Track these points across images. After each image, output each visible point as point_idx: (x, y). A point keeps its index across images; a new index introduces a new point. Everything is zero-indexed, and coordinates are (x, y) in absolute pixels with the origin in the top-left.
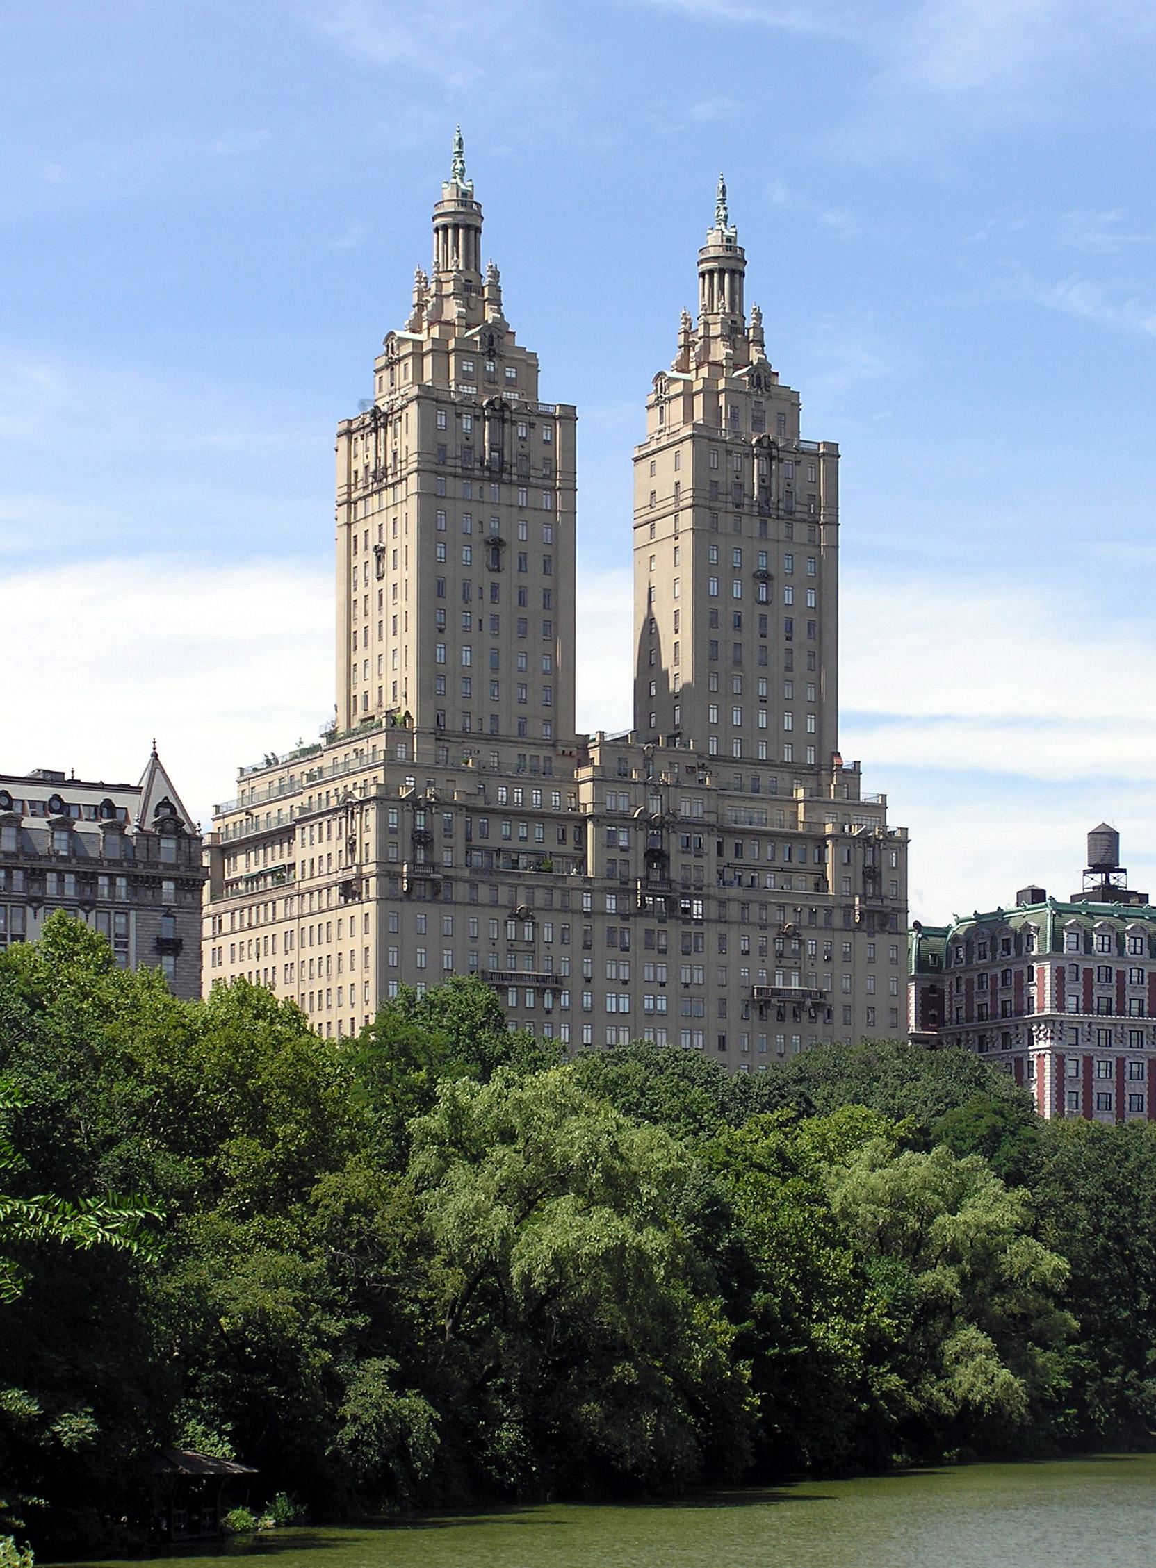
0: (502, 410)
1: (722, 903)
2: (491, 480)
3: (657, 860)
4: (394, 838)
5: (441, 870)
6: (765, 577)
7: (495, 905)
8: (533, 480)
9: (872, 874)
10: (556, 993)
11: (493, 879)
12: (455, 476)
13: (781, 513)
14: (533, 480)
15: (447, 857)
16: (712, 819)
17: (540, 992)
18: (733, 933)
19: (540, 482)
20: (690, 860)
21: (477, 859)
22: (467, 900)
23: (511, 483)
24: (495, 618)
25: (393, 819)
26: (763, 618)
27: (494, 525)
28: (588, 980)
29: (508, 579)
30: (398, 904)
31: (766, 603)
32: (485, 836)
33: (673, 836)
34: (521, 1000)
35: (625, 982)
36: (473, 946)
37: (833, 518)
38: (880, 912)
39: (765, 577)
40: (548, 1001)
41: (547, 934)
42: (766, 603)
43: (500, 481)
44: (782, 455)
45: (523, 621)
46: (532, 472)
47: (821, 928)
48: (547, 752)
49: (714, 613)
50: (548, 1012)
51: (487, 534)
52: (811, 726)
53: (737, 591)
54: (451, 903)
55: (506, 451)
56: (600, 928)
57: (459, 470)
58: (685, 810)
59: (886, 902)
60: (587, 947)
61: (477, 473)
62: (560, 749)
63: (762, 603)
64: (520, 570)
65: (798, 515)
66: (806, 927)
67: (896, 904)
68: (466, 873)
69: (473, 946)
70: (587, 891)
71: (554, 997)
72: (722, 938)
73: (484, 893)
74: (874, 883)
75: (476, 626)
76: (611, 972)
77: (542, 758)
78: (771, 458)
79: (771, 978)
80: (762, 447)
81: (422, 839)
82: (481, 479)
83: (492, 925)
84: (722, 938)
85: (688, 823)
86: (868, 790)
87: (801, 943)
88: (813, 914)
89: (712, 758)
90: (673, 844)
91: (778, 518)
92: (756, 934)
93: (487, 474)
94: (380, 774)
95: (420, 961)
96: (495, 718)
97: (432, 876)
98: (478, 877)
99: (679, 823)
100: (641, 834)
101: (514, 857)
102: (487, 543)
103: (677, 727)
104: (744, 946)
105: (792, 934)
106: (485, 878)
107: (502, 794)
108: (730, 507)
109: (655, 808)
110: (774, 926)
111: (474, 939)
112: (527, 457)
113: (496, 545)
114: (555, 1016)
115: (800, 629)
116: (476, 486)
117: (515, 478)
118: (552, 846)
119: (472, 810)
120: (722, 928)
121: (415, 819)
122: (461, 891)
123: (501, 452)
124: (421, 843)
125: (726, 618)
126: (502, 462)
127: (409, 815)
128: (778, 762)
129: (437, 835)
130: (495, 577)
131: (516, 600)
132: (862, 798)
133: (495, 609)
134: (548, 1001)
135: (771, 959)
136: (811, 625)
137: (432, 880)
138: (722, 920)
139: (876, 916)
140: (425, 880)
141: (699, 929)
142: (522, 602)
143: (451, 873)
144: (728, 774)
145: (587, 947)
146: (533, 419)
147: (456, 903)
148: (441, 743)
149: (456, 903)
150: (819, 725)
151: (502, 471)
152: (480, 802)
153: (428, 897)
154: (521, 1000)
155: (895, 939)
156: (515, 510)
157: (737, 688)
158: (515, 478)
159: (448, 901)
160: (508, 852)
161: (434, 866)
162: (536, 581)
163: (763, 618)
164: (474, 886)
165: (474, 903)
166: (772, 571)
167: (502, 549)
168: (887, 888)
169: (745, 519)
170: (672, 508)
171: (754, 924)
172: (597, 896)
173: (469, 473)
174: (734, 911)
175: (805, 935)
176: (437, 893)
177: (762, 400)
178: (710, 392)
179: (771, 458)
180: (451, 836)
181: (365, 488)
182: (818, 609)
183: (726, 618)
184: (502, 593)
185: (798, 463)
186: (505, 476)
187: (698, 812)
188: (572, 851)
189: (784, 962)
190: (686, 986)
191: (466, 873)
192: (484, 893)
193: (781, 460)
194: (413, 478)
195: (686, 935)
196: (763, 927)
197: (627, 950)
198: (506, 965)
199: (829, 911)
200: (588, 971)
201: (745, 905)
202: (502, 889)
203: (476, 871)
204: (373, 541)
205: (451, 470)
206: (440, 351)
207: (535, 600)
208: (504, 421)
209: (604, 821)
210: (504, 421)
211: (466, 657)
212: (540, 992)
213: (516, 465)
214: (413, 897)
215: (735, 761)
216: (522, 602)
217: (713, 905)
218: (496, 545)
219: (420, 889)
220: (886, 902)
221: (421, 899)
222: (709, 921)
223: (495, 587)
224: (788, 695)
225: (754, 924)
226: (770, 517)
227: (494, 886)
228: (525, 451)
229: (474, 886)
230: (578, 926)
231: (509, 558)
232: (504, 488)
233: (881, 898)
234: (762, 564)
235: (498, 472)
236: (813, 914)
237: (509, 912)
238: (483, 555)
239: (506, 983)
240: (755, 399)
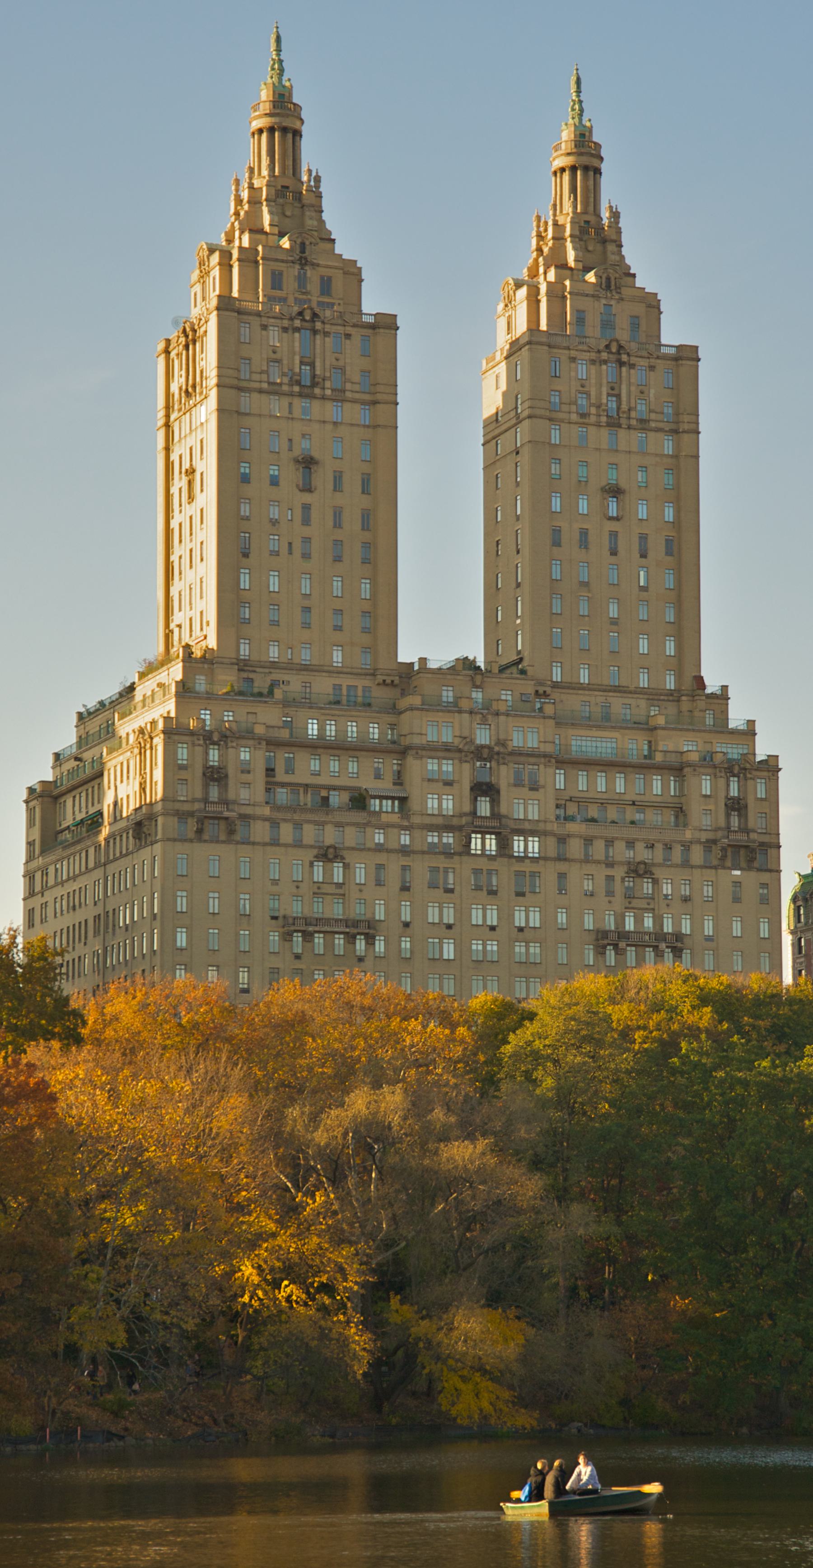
0: (313, 321)
1: (562, 840)
2: (301, 395)
3: (485, 794)
4: (184, 775)
5: (236, 807)
6: (615, 491)
7: (298, 844)
8: (348, 395)
9: (737, 806)
10: (370, 940)
11: (296, 817)
12: (261, 391)
13: (634, 422)
14: (348, 395)
15: (244, 794)
16: (548, 748)
17: (351, 939)
18: (574, 873)
19: (357, 396)
21: (282, 795)
22: (267, 839)
23: (323, 398)
24: (307, 540)
25: (183, 753)
26: (614, 535)
27: (305, 444)
28: (407, 925)
29: (322, 499)
30: (187, 845)
31: (617, 519)
32: (290, 770)
33: (503, 768)
34: (329, 946)
35: (449, 927)
36: (275, 889)
37: (692, 426)
38: (746, 847)
39: (615, 491)
40: (360, 945)
41: (360, 875)
42: (617, 519)
43: (313, 397)
44: (633, 360)
45: (338, 543)
46: (348, 386)
47: (677, 866)
48: (367, 682)
49: (557, 532)
50: (361, 959)
51: (297, 452)
52: (670, 648)
53: (583, 506)
54: (249, 843)
55: (318, 364)
56: (421, 869)
57: (265, 386)
58: (517, 740)
59: (753, 836)
60: (405, 888)
61: (285, 388)
62: (380, 678)
63: (611, 519)
64: (335, 490)
65: (653, 425)
66: (659, 865)
67: (766, 839)
68: (267, 811)
69: (275, 889)
70: (405, 828)
71: (367, 943)
72: (562, 876)
73: (286, 832)
74: (739, 816)
75: (284, 550)
76: (433, 915)
77: (360, 689)
78: (621, 364)
79: (620, 919)
80: (610, 353)
81: (215, 776)
82: (291, 394)
83: (292, 867)
84: (562, 876)
85: (517, 753)
86: (736, 718)
87: (655, 882)
88: (668, 847)
89: (556, 685)
90: (504, 776)
91: (629, 427)
92: (602, 873)
93: (296, 389)
94: (170, 707)
95: (214, 906)
97: (226, 814)
98: (280, 815)
99: (511, 754)
100: (466, 767)
101: (324, 793)
102: (297, 461)
103: (519, 652)
104: (588, 886)
105: (639, 871)
106: (288, 816)
107: (313, 729)
108: (574, 417)
109: (483, 737)
110: (621, 863)
111: (275, 882)
112: (343, 370)
113: (308, 463)
114: (369, 963)
117: (328, 392)
118: (367, 783)
119: (273, 744)
120: (562, 867)
121: (207, 754)
122: (260, 831)
123: (312, 365)
124: (214, 780)
125: (571, 535)
126: (314, 376)
127: (199, 750)
128: (632, 688)
129: (231, 772)
130: (307, 498)
131: (331, 523)
132: (730, 727)
133: (306, 531)
134: (360, 945)
135: (618, 900)
136: (669, 542)
137: (227, 819)
138: (561, 858)
139: (742, 852)
140: (219, 818)
141: (535, 868)
142: (338, 524)
143: (248, 810)
144: (572, 702)
145: (405, 888)
146: (349, 330)
147: (254, 844)
148: (245, 675)
149: (254, 844)
150: (679, 647)
151: (314, 384)
152: (285, 734)
153: (223, 837)
154: (329, 946)
155: (765, 877)
156: (329, 427)
157: (584, 609)
158: (328, 392)
159: (247, 842)
161: (225, 802)
162: (353, 501)
163: (614, 535)
164: (275, 824)
165: (275, 842)
166: (623, 484)
167: (314, 468)
168: (754, 821)
169: (592, 430)
170: (514, 421)
171: (598, 862)
172: (417, 833)
173: (276, 388)
174: (575, 848)
175: (658, 872)
176: (231, 832)
177: (613, 302)
178: (556, 294)
179: (621, 364)
180: (249, 772)
181: (180, 410)
182: (677, 524)
183: (571, 535)
184: (315, 515)
185: (652, 368)
186: (317, 391)
187: (532, 742)
188: (391, 786)
189: (636, 903)
190: (521, 929)
191: (267, 811)
192: (286, 832)
193: (632, 366)
194: (213, 394)
195: (518, 874)
196: (610, 865)
197: (452, 891)
198: (318, 909)
199: (687, 846)
200: (406, 916)
201: (588, 841)
202: (306, 827)
203: (277, 808)
204: (186, 465)
205: (256, 385)
206: (248, 258)
207: (352, 522)
208: (315, 332)
209: (424, 753)
210: (315, 332)
211: (274, 584)
212: (351, 939)
213: (330, 378)
214: (206, 837)
215: (581, 687)
216: (338, 524)
217: (551, 841)
218: (308, 463)
219: (210, 829)
220: (753, 836)
222: (545, 859)
223: (306, 508)
224: (643, 615)
225: (598, 862)
226: (620, 426)
227: (298, 826)
228: (341, 363)
229: (275, 824)
230: (394, 865)
231: (323, 478)
232: (316, 404)
233: (745, 830)
234: (612, 476)
235: (308, 387)
236: (668, 847)
237: (315, 852)
238: (291, 476)
239: (311, 929)
240: (604, 301)
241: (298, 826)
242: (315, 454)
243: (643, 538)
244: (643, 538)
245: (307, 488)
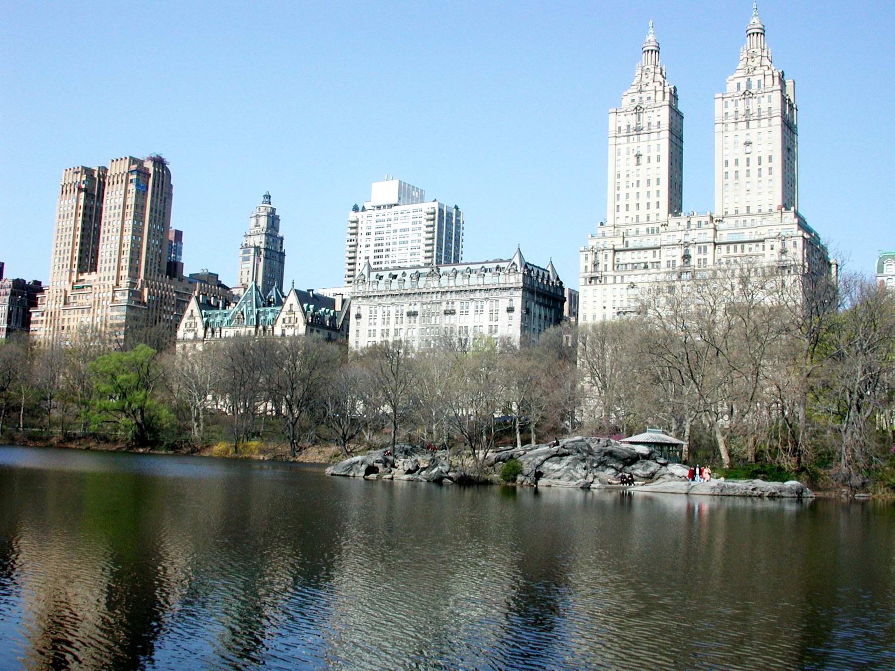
6: (747, 144)
7: (622, 282)
20: (702, 256)
26: (748, 159)
39: (747, 144)
90: (693, 251)
96: (638, 217)
115: (765, 160)
116: (631, 138)
122: (610, 280)
159: (605, 283)
160: (633, 264)
163: (748, 159)
164: (615, 277)
218: (638, 156)
221: (596, 284)
231: (643, 160)
241: (622, 277)
242: (641, 153)
243: (760, 158)
244: (760, 158)
245: (638, 164)
